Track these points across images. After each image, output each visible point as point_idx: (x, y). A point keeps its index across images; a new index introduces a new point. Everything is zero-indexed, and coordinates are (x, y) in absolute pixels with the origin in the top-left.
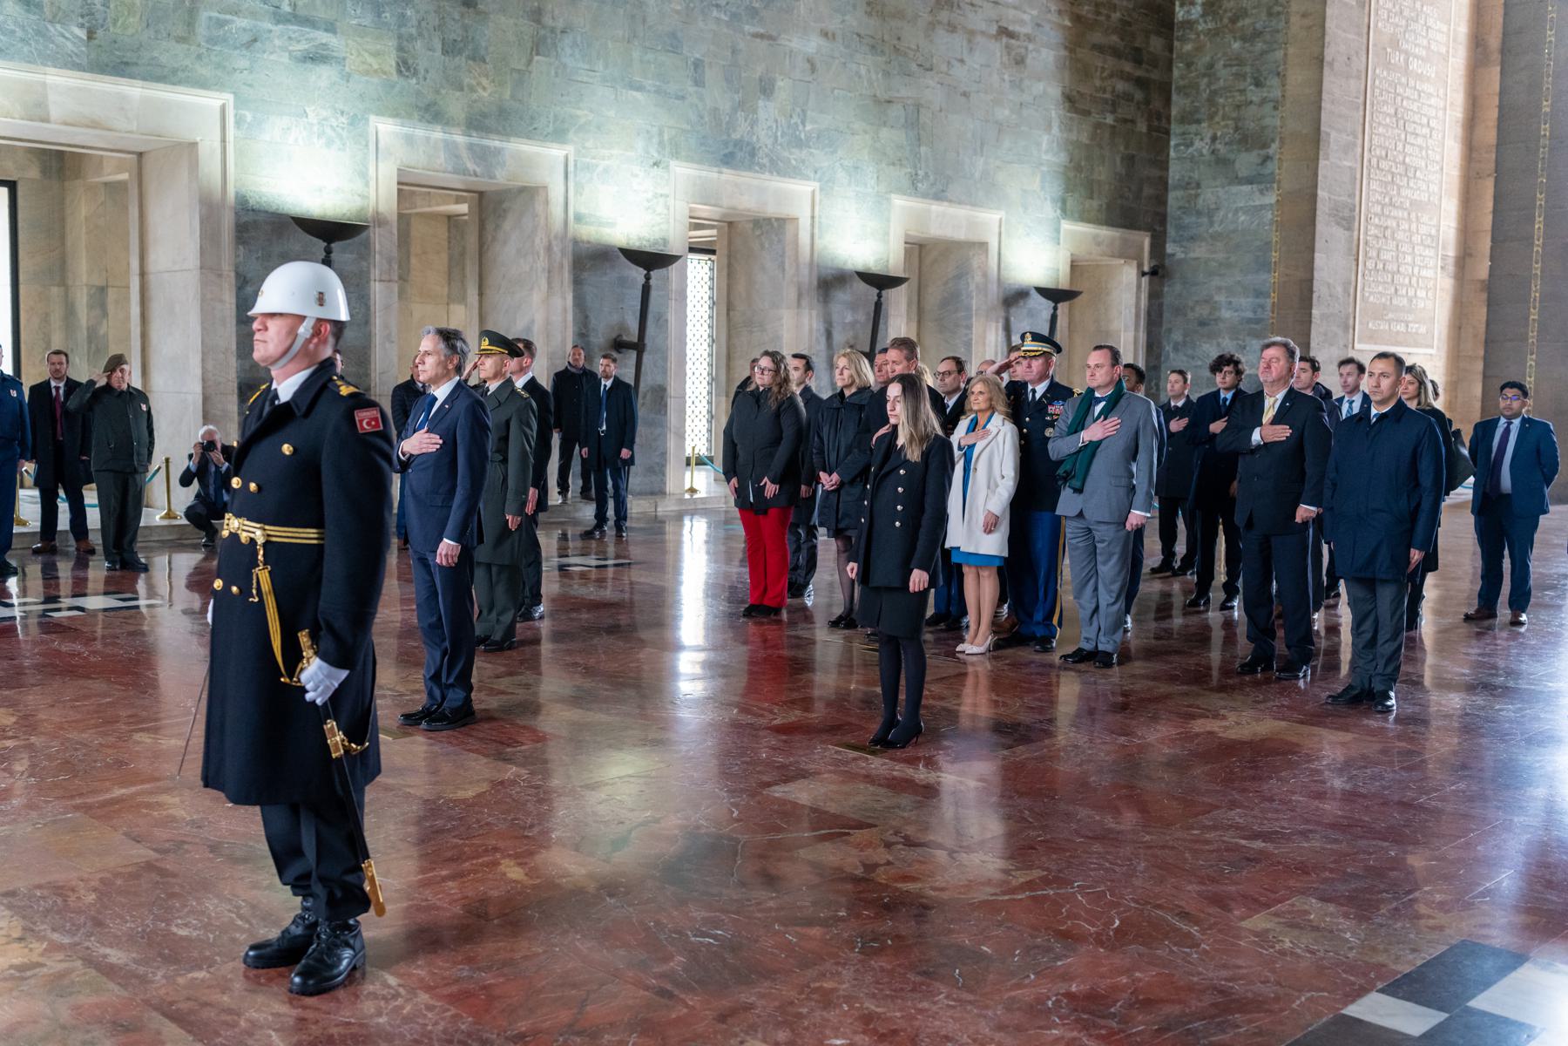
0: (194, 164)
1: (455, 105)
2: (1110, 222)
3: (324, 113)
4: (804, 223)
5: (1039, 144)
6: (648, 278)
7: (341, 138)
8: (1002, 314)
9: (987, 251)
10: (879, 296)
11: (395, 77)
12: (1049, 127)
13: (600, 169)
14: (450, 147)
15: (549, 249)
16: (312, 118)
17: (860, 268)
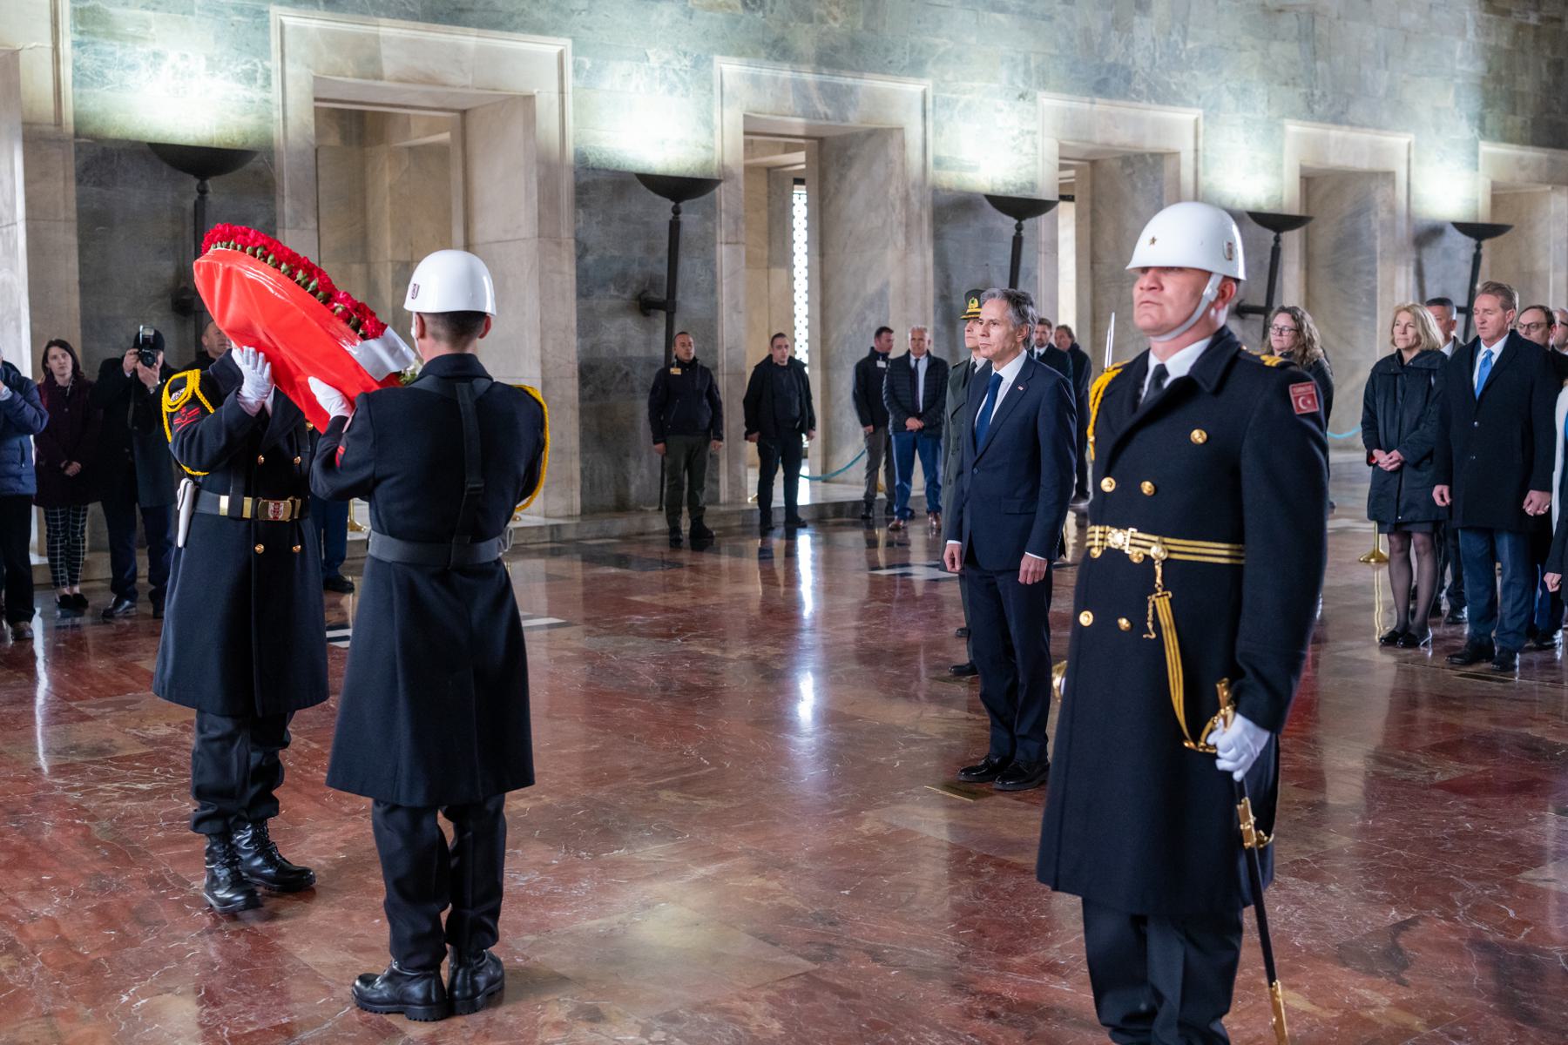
0: (530, 120)
1: (804, 39)
2: (1536, 142)
3: (666, 56)
4: (1187, 158)
5: (1451, 53)
6: (1019, 228)
7: (683, 81)
8: (1413, 256)
9: (1393, 182)
10: (1277, 240)
11: (740, 11)
12: (1462, 33)
13: (961, 104)
14: (800, 87)
15: (906, 199)
16: (654, 61)
17: (1251, 208)
